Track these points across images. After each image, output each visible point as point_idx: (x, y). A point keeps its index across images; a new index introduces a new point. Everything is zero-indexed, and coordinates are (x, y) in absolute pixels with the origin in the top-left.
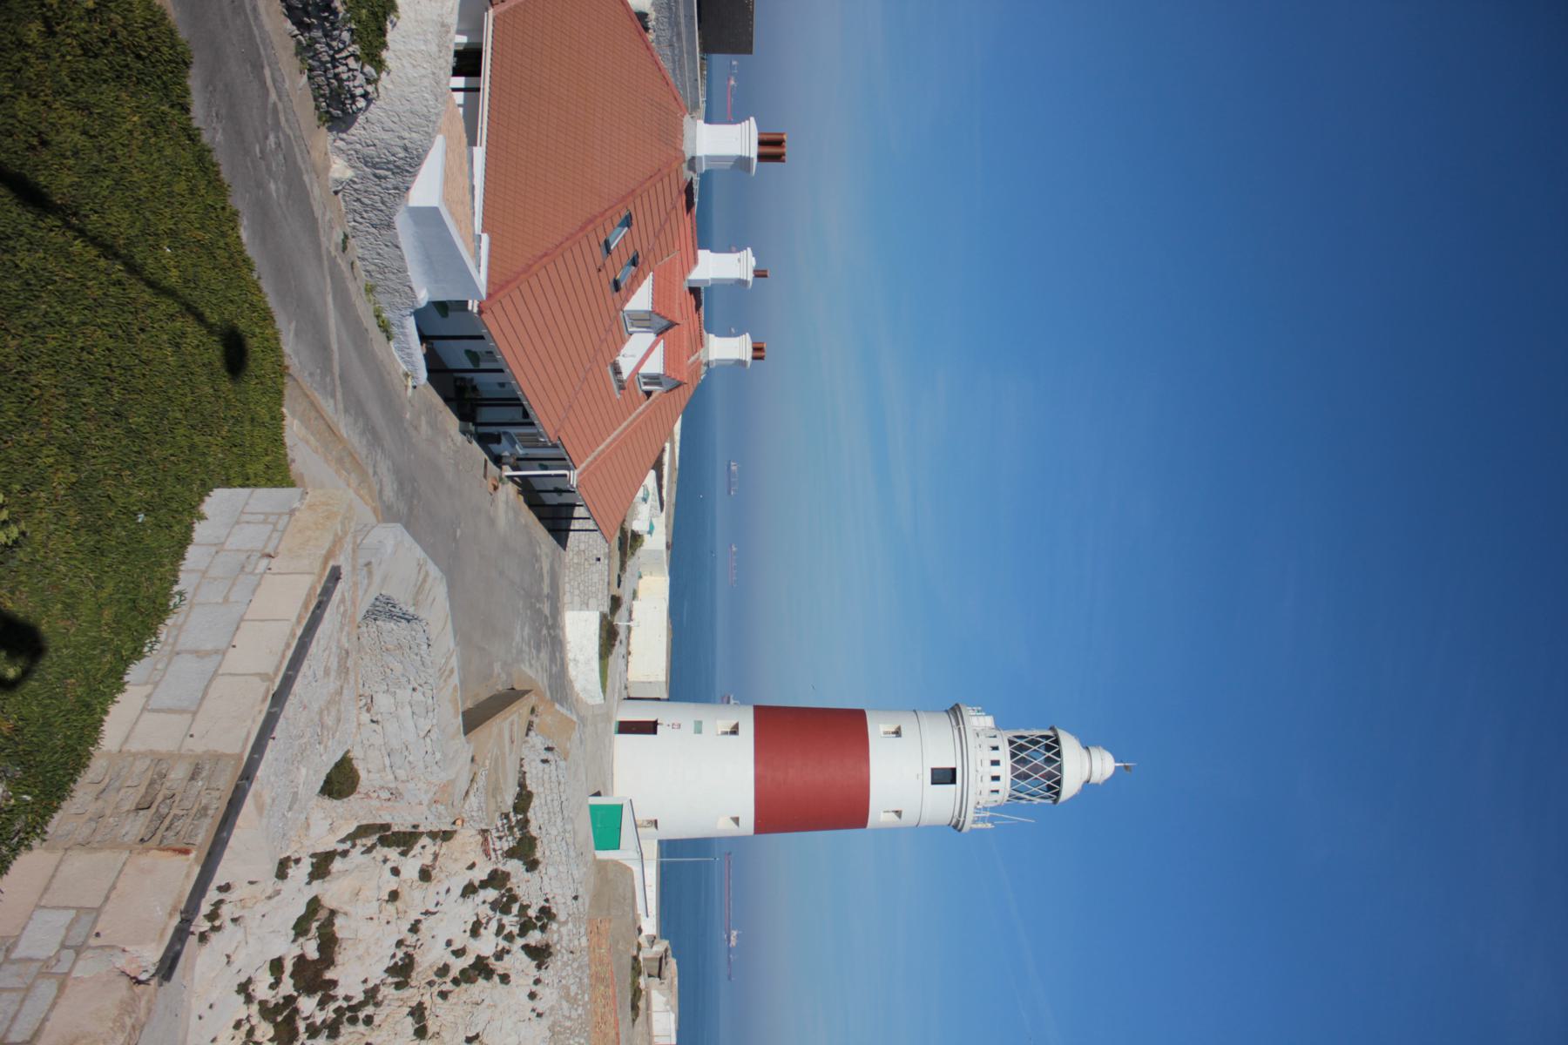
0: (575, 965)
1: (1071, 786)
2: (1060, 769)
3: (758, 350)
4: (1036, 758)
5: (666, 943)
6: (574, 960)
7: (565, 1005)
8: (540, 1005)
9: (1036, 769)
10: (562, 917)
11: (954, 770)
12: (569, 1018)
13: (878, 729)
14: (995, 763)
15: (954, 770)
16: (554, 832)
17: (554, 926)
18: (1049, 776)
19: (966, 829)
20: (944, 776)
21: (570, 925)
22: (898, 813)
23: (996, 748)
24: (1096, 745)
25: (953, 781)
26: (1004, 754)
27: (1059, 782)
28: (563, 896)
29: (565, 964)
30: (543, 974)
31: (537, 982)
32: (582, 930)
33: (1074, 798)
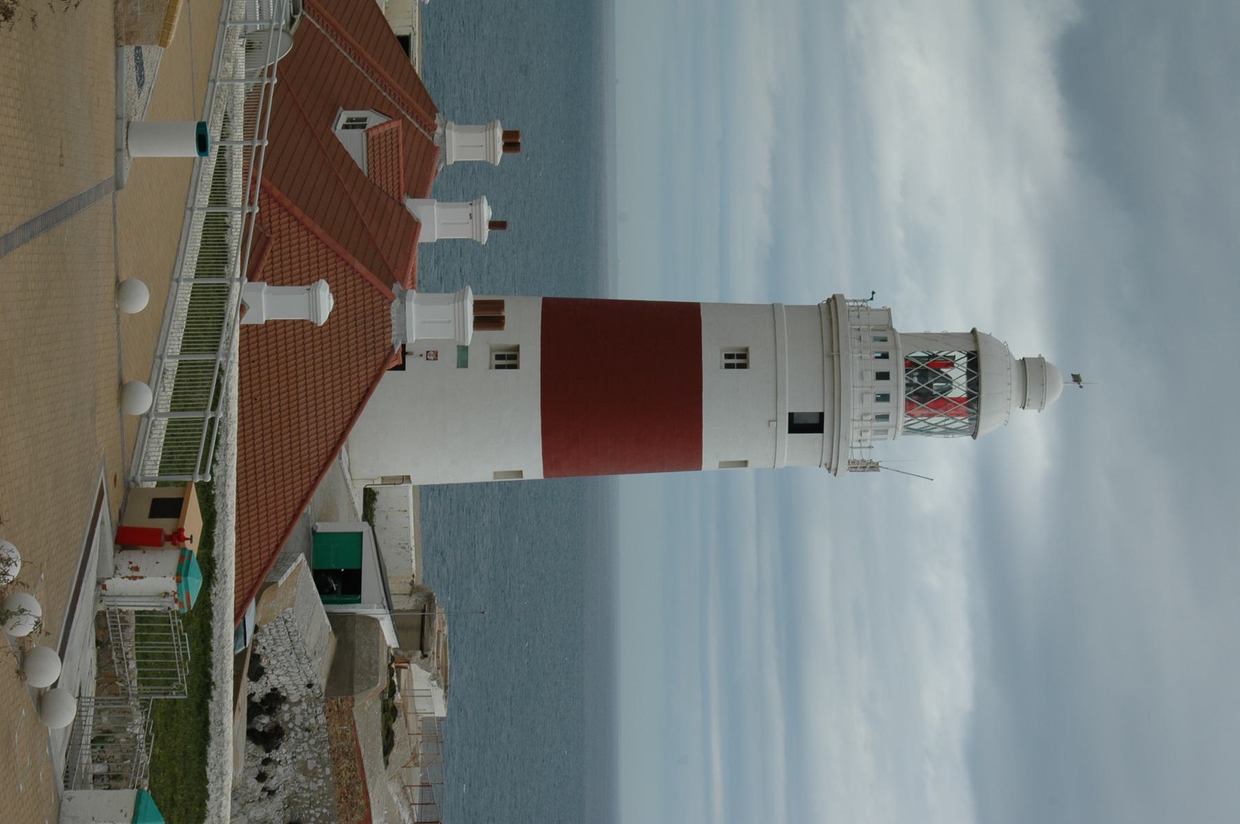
0: (312, 742)
3: (511, 142)
6: (310, 737)
7: (302, 778)
8: (272, 784)
11: (822, 415)
12: (308, 790)
17: (285, 707)
21: (304, 705)
23: (883, 376)
26: (900, 378)
29: (299, 742)
30: (275, 755)
31: (266, 762)
32: (320, 709)
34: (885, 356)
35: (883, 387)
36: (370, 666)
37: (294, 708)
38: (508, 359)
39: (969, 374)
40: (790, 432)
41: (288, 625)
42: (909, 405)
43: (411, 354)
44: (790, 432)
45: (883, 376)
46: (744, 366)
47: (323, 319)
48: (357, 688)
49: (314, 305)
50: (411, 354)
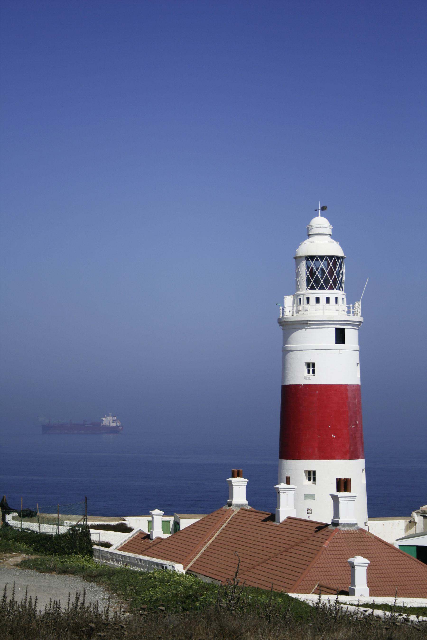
1: (334, 249)
2: (331, 257)
4: (323, 274)
5: (414, 514)
9: (331, 273)
11: (336, 329)
13: (299, 377)
14: (328, 300)
15: (336, 329)
18: (335, 265)
19: (361, 319)
20: (340, 336)
22: (358, 364)
23: (318, 300)
24: (308, 230)
25: (343, 329)
26: (317, 293)
27: (338, 258)
33: (342, 245)
34: (308, 299)
35: (323, 300)
38: (311, 475)
39: (317, 260)
40: (343, 343)
44: (343, 343)
45: (318, 300)
46: (314, 365)
47: (367, 561)
49: (361, 565)
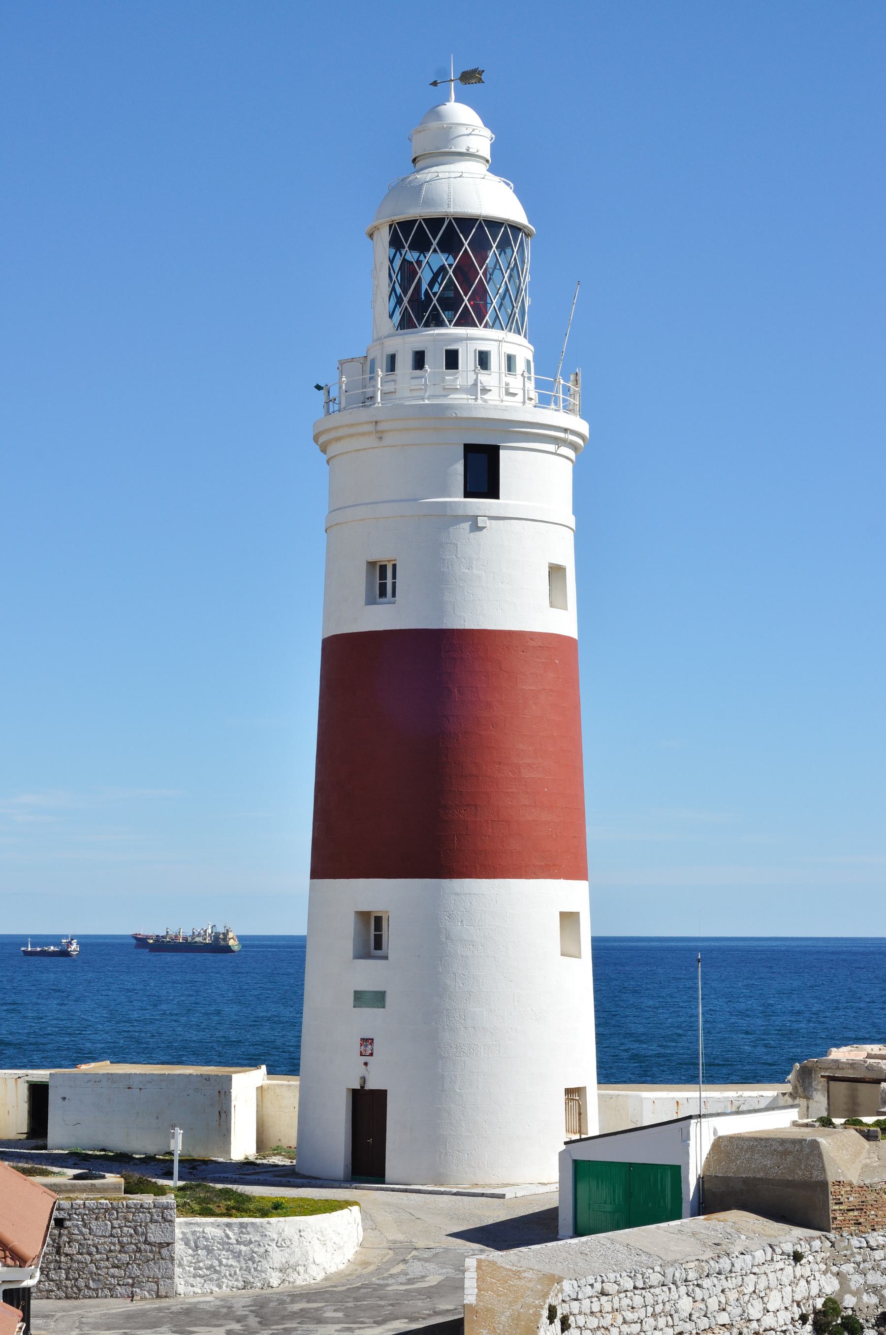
10: (831, 1286)
16: (685, 1305)
17: (849, 1301)
23: (419, 360)
27: (494, 224)
28: (794, 1283)
32: (855, 1242)
36: (786, 1153)
37: (853, 1286)
41: (611, 1288)
42: (465, 321)
43: (364, 1080)
45: (419, 360)
48: (816, 1176)
50: (364, 1080)
